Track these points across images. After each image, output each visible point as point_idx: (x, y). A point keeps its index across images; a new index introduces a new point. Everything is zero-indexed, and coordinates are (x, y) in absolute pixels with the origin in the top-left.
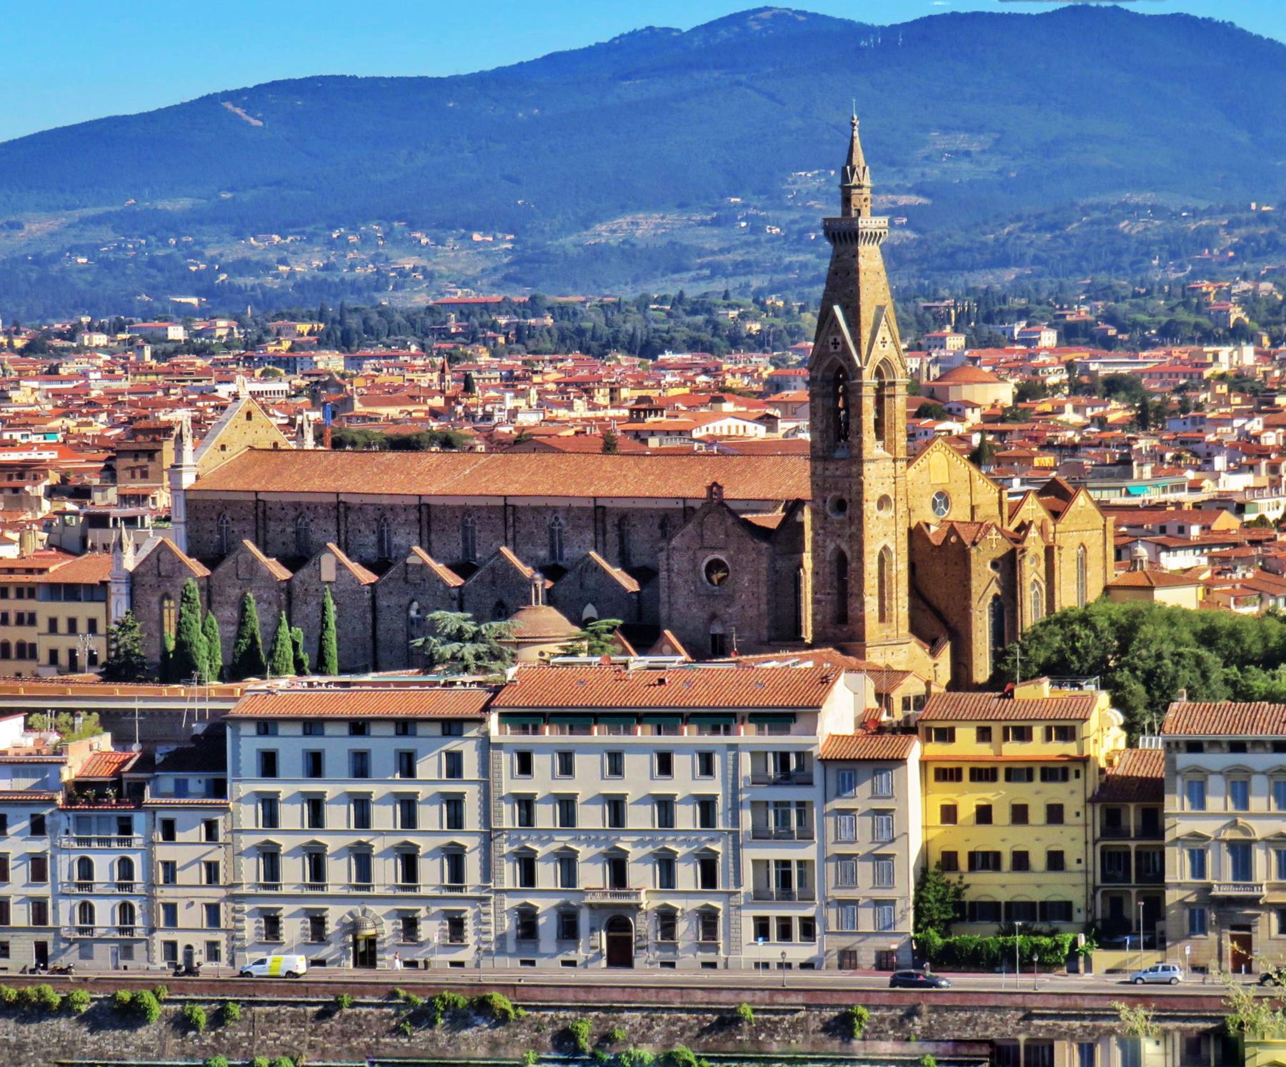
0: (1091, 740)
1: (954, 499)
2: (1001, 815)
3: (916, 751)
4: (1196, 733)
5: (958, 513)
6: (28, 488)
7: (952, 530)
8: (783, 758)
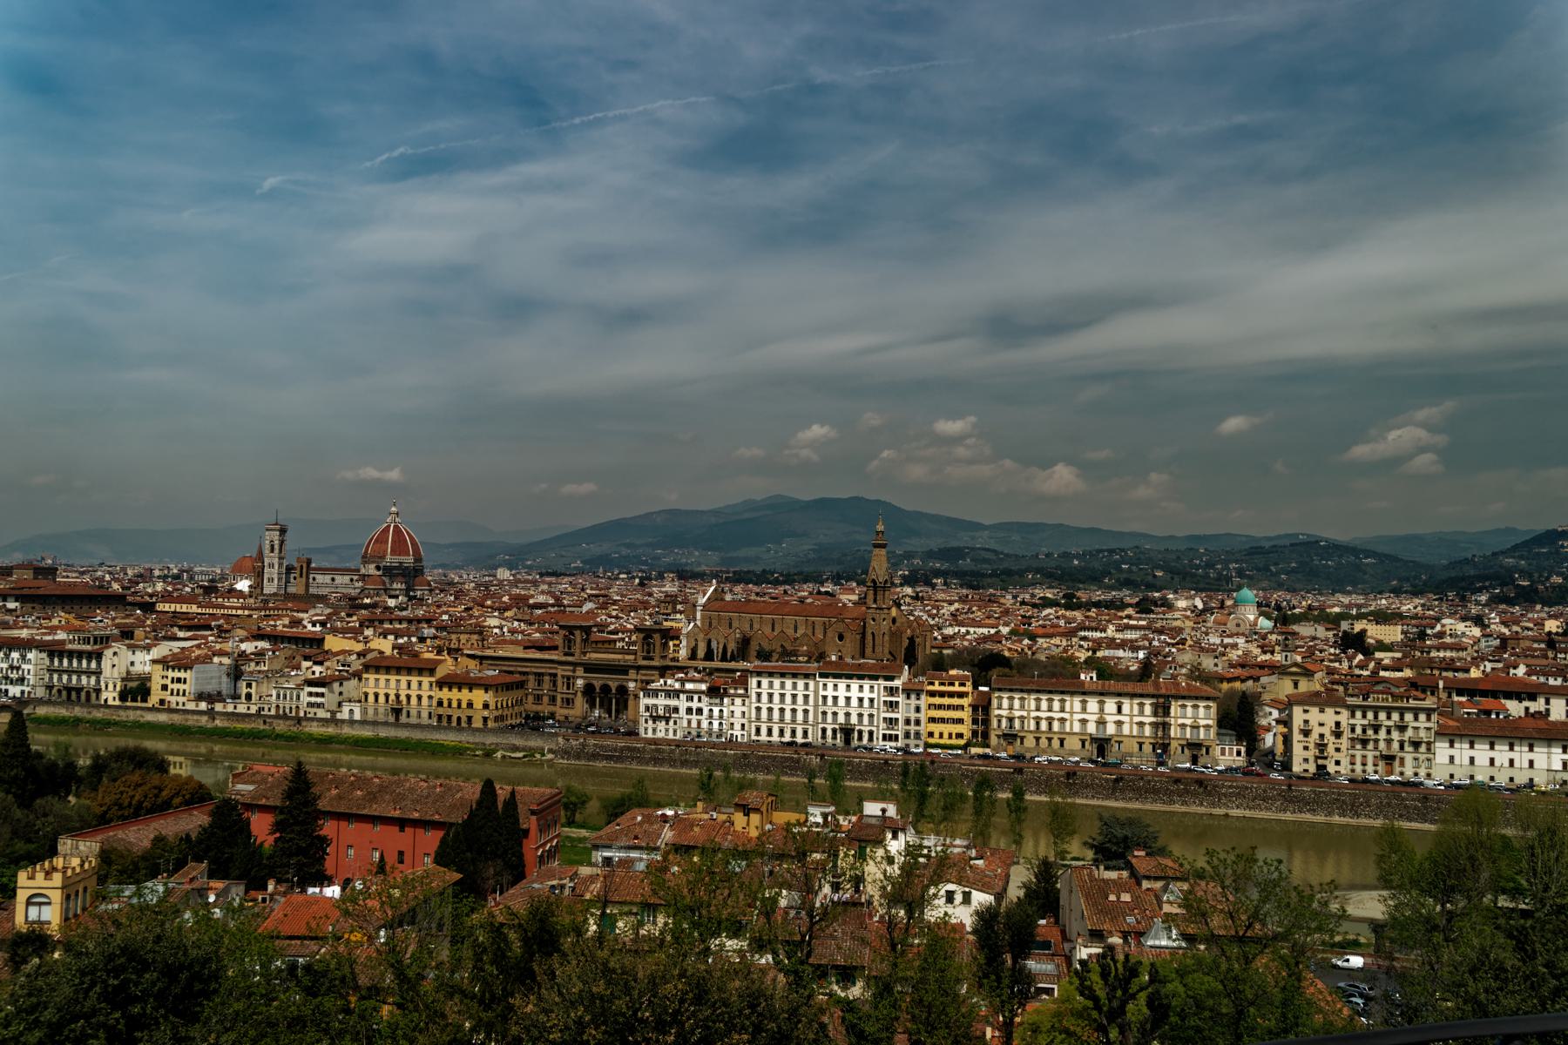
8: (891, 688)
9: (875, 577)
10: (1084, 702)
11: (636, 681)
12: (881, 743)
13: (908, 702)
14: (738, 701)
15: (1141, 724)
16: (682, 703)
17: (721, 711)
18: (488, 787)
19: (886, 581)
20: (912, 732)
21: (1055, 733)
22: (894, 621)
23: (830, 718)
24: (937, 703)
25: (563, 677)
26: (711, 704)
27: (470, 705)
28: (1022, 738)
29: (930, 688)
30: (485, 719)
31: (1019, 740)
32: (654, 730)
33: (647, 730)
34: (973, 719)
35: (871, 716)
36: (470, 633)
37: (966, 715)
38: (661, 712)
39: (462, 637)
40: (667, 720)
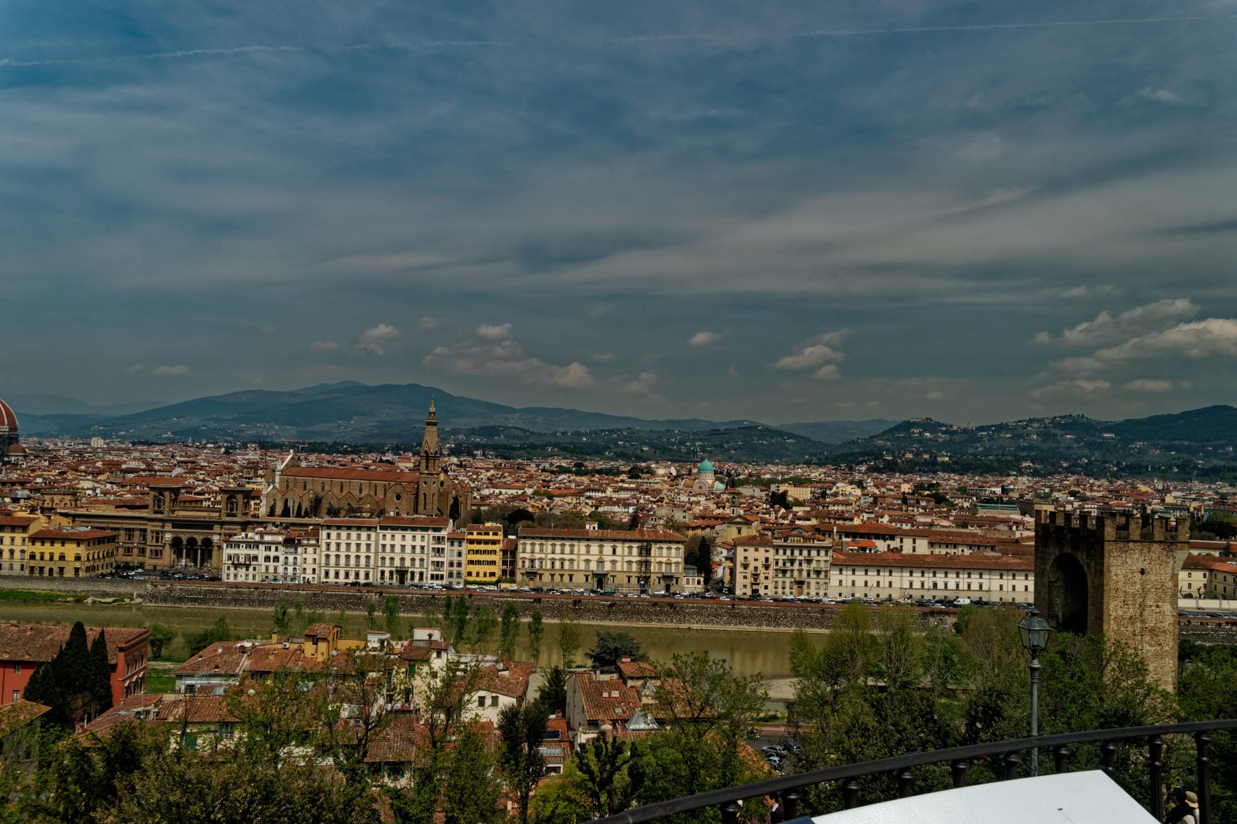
8: (439, 538)
9: (427, 449)
10: (588, 546)
11: (220, 534)
12: (430, 581)
13: (452, 548)
14: (310, 550)
15: (630, 562)
16: (261, 553)
17: (295, 558)
18: (79, 629)
19: (436, 452)
20: (455, 572)
21: (566, 570)
22: (442, 484)
23: (388, 562)
24: (475, 549)
25: (152, 532)
26: (286, 553)
27: (62, 557)
28: (541, 575)
29: (470, 537)
30: (77, 570)
31: (538, 577)
32: (236, 576)
33: (230, 576)
34: (503, 561)
35: (422, 560)
36: (64, 495)
37: (498, 558)
38: (242, 561)
39: (55, 497)
40: (247, 567)
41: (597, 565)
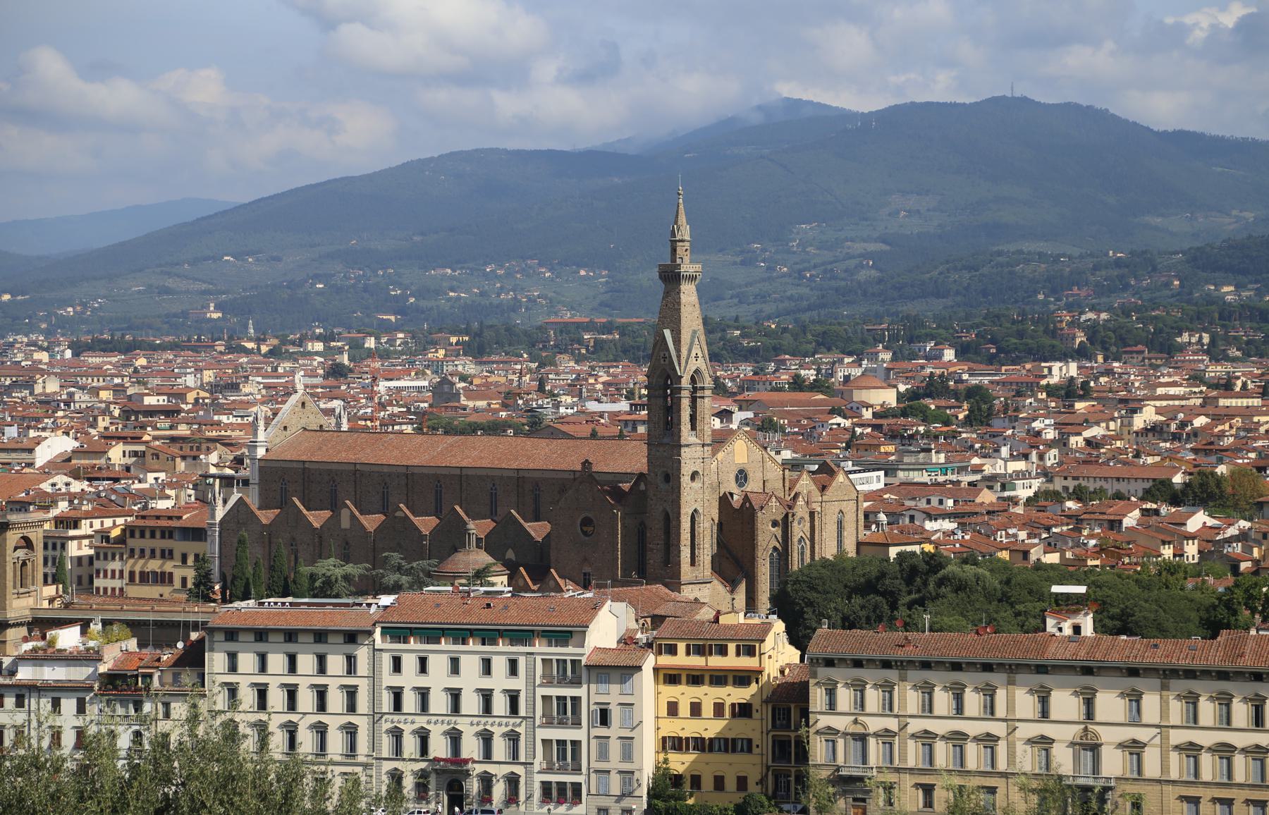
0: (767, 655)
1: (750, 475)
2: (684, 710)
3: (650, 662)
4: (830, 652)
5: (753, 486)
6: (202, 457)
7: (746, 498)
15: (1192, 750)
23: (410, 745)
35: (513, 738)
41: (1076, 759)
